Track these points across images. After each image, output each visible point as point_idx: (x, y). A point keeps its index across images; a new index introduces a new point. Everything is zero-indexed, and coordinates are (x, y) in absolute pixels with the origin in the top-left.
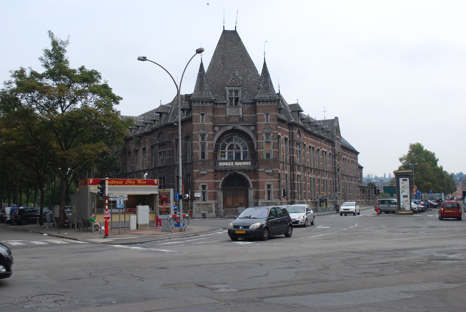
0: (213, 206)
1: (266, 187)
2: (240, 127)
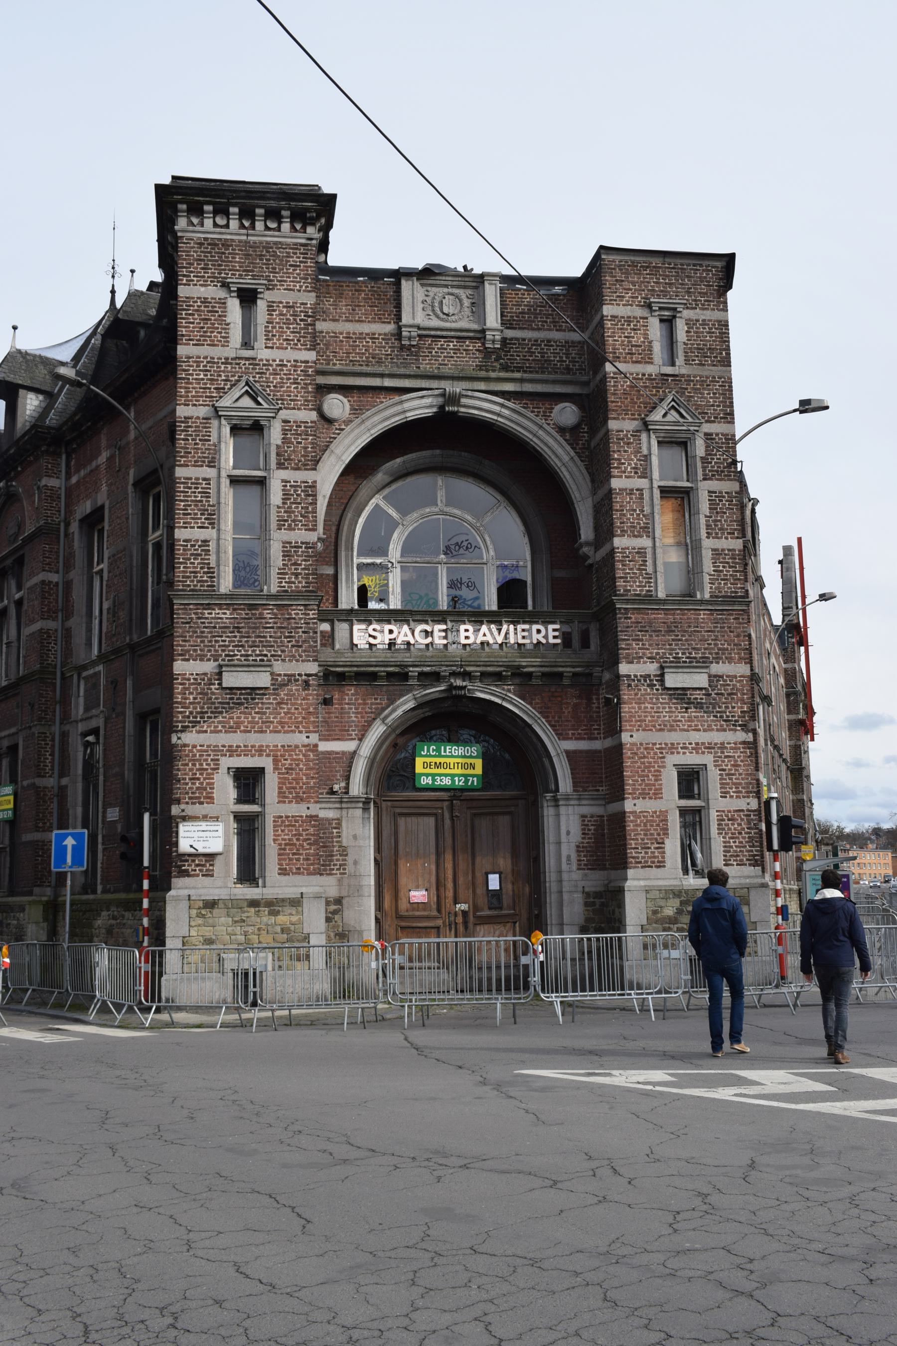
0: (314, 920)
1: (670, 782)
2: (483, 405)
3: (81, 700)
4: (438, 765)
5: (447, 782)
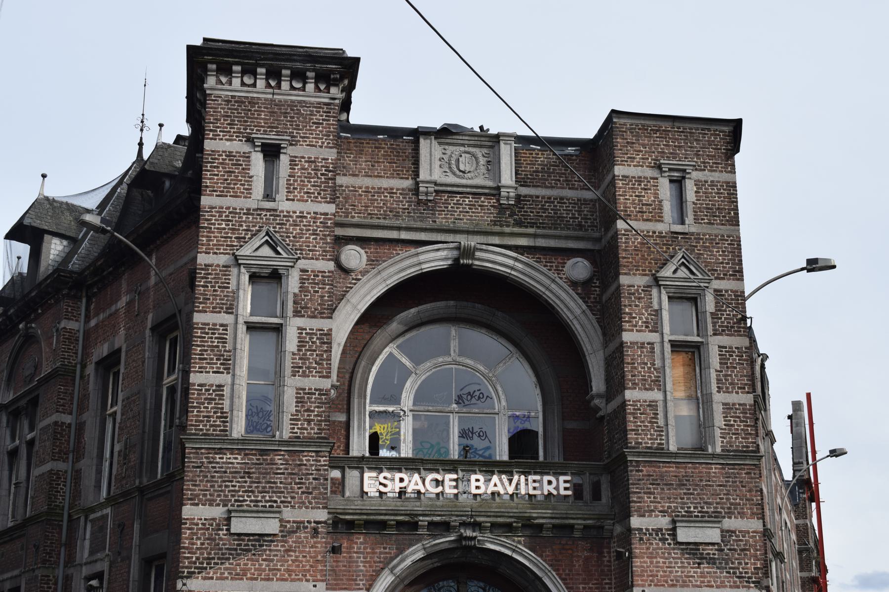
2: (497, 259)
3: (87, 543)
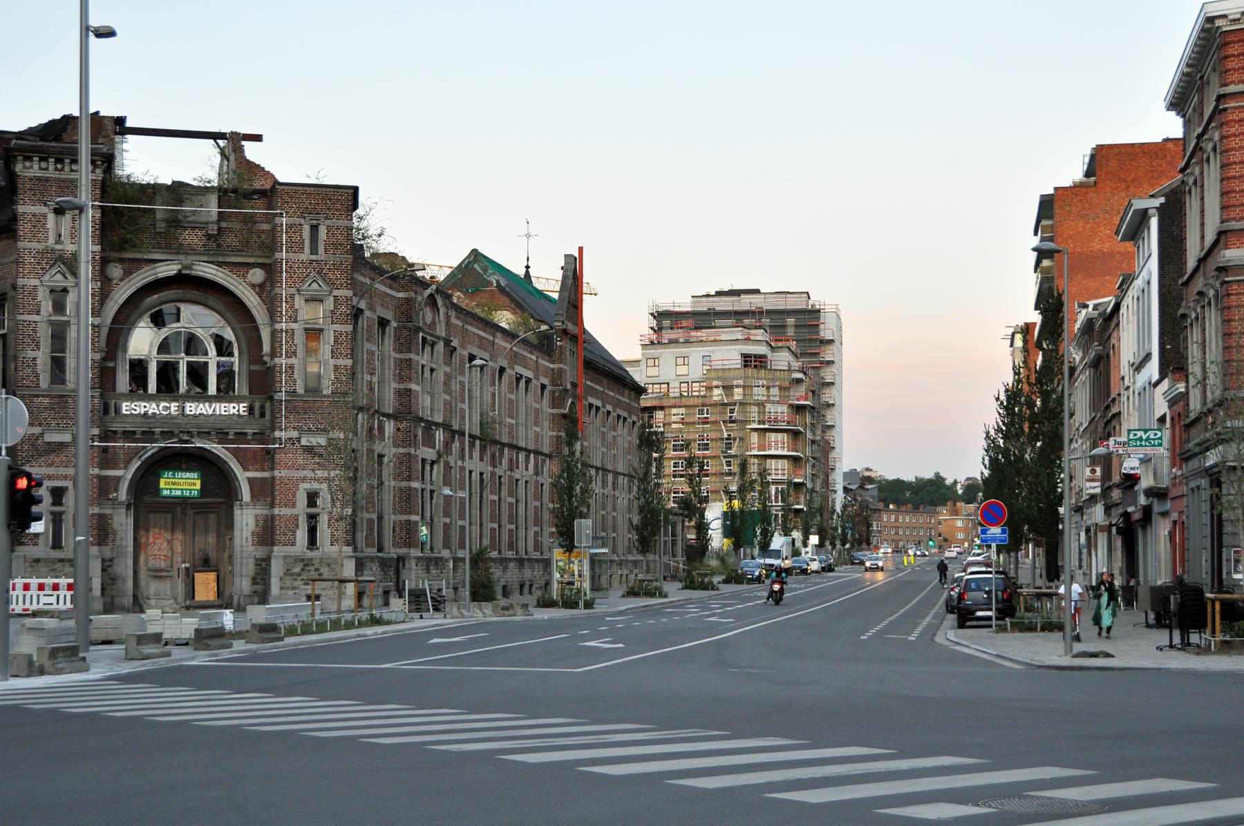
1: (302, 500)
4: (174, 484)
5: (179, 493)
